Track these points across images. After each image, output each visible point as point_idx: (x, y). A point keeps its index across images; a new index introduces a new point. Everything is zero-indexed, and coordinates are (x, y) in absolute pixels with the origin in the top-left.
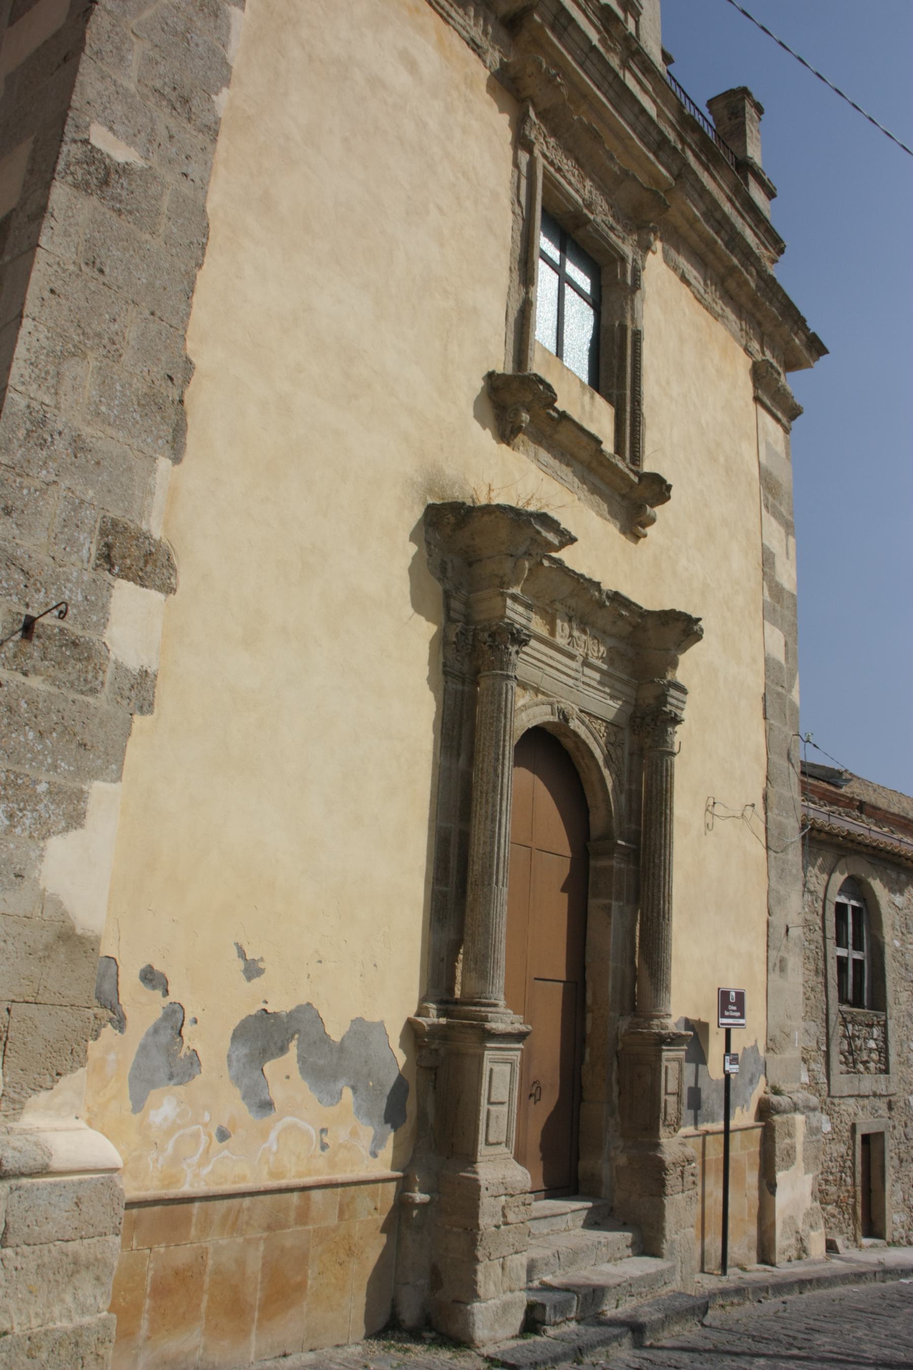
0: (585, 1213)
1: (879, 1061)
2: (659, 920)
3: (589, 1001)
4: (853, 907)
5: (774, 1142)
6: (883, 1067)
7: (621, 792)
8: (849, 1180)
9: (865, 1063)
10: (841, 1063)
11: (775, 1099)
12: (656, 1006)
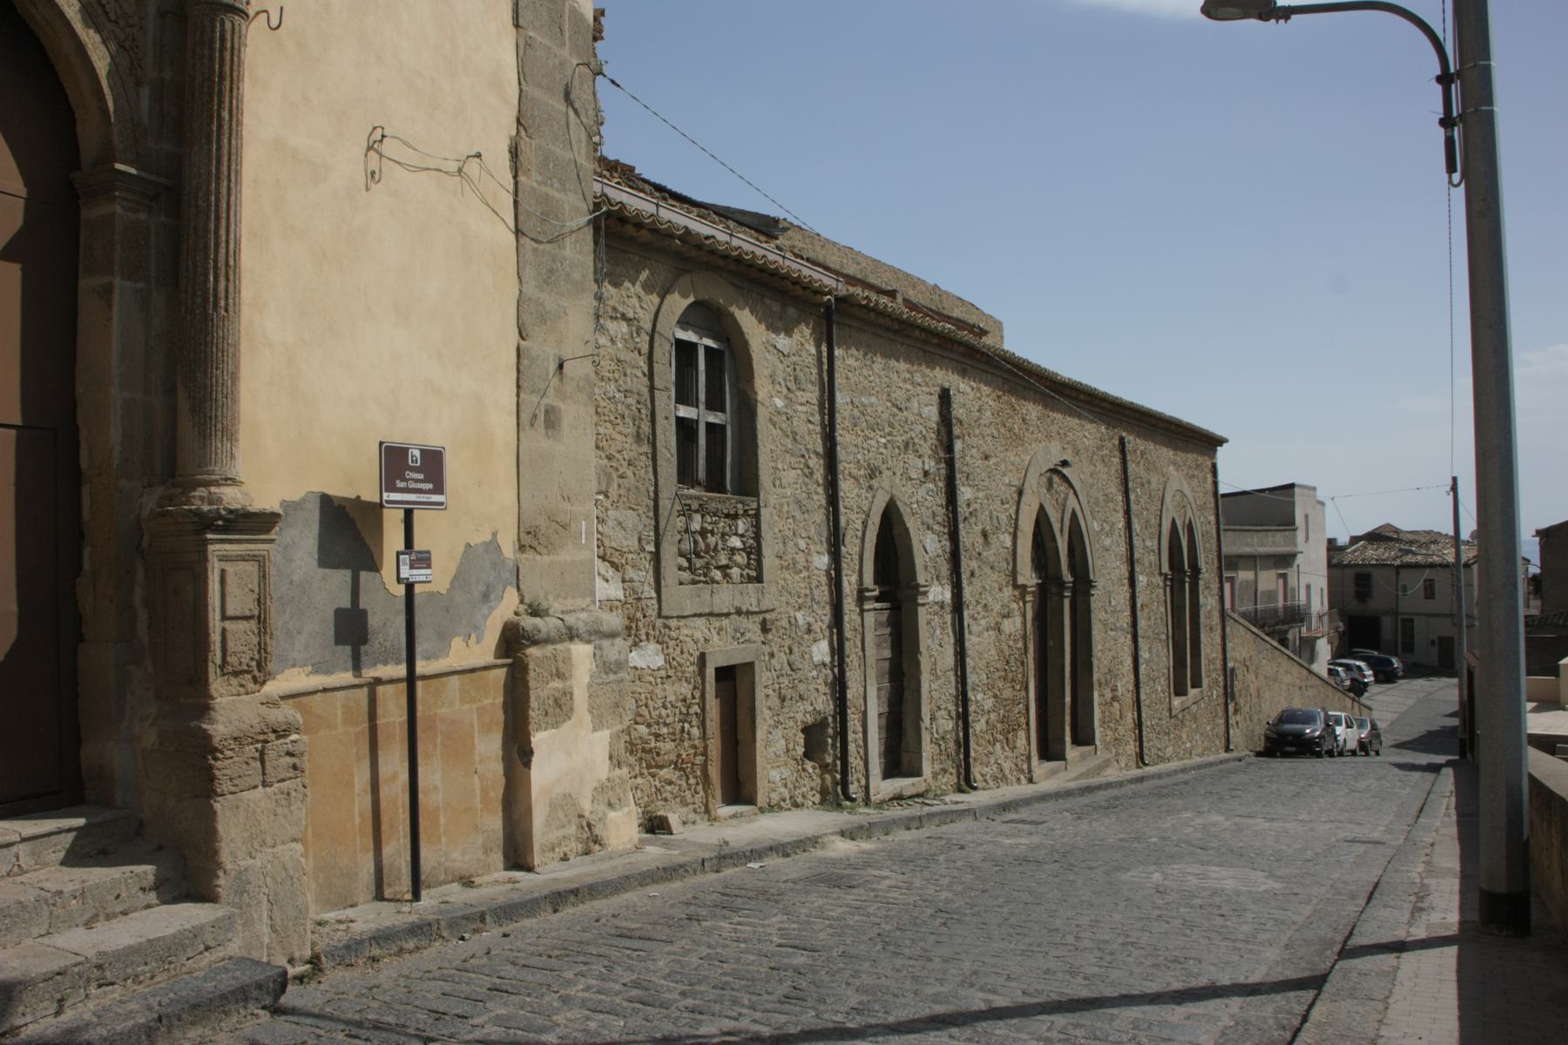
0: (71, 837)
1: (748, 566)
2: (206, 309)
3: (84, 464)
4: (707, 348)
5: (527, 688)
6: (754, 574)
7: (138, 84)
8: (696, 732)
9: (724, 569)
10: (680, 568)
11: (528, 622)
12: (203, 463)
